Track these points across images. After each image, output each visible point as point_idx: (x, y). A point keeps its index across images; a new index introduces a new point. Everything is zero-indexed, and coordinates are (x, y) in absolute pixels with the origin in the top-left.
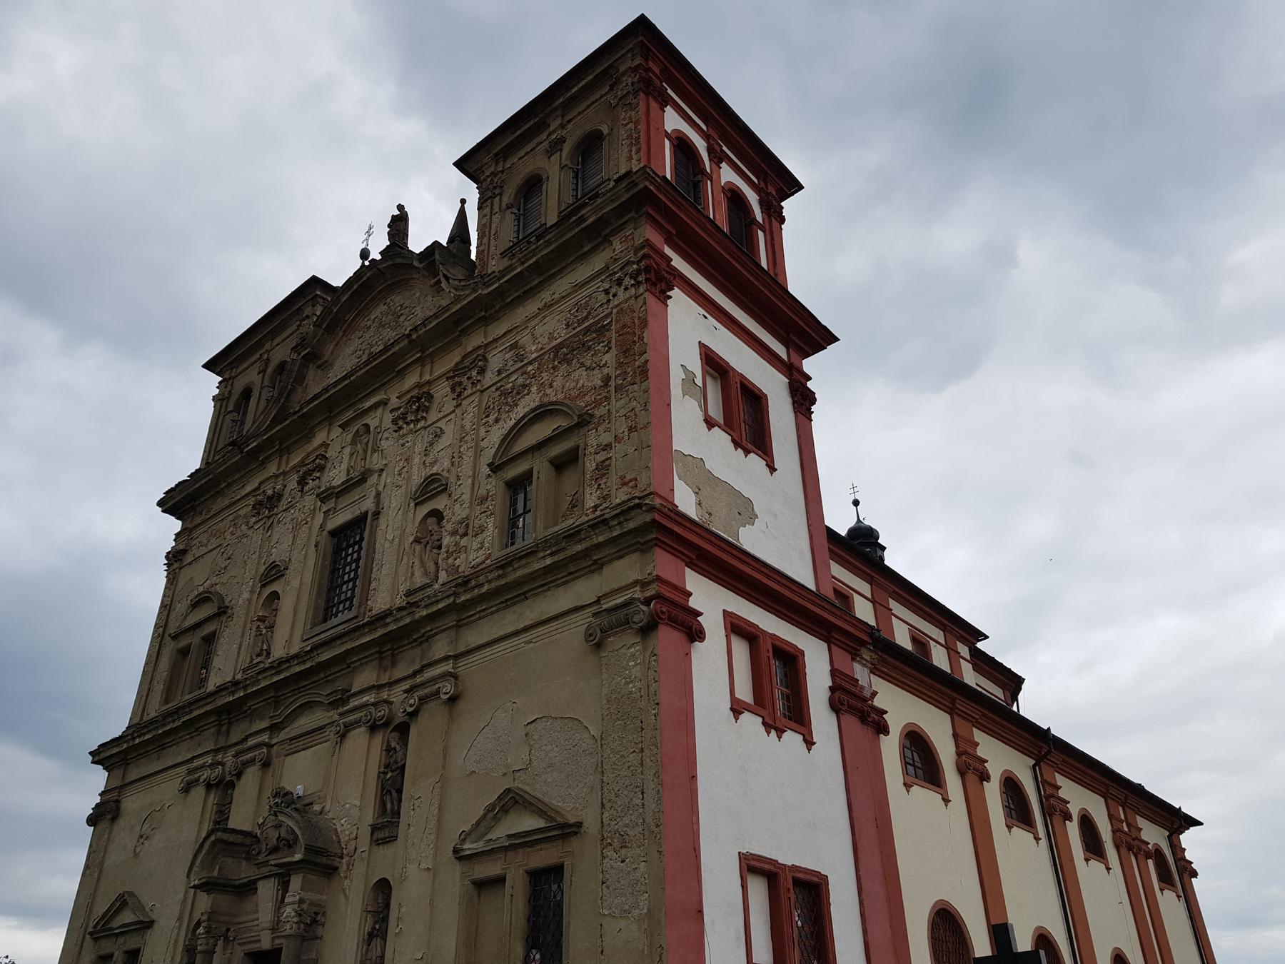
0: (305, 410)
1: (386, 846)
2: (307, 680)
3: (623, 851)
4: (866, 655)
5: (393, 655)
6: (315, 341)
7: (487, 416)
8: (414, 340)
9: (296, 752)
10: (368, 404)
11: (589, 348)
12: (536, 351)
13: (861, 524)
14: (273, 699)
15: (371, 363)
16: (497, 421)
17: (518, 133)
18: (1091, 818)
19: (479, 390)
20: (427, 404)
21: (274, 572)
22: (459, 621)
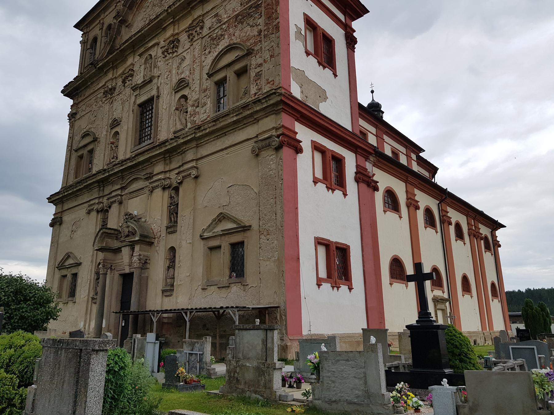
0: (122, 48)
1: (173, 234)
2: (134, 169)
3: (268, 236)
4: (372, 158)
5: (170, 159)
6: (124, 13)
7: (205, 50)
8: (169, 13)
9: (133, 198)
10: (150, 44)
11: (252, 16)
12: (227, 17)
13: (374, 102)
14: (121, 177)
15: (150, 24)
16: (210, 52)
18: (393, 192)
19: (201, 37)
20: (177, 44)
21: (115, 123)
22: (197, 145)
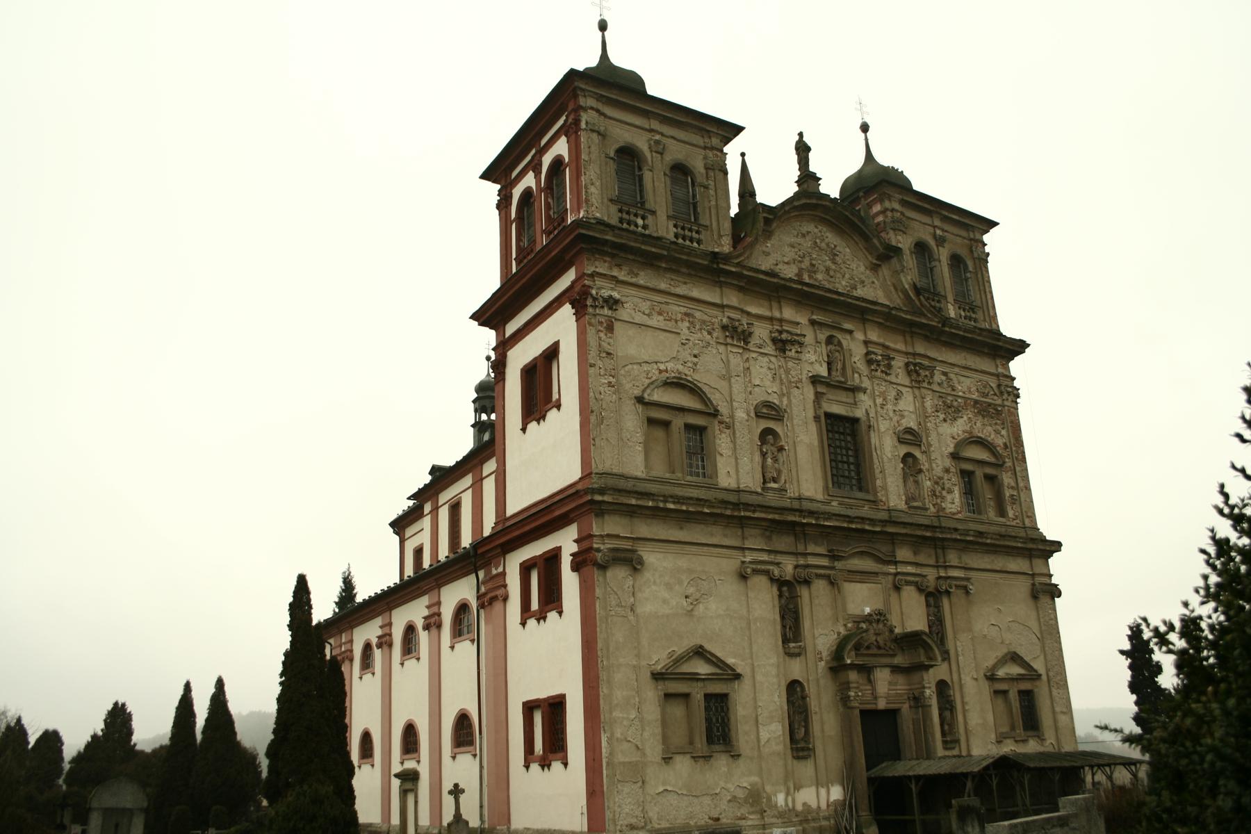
17: (920, 203)
